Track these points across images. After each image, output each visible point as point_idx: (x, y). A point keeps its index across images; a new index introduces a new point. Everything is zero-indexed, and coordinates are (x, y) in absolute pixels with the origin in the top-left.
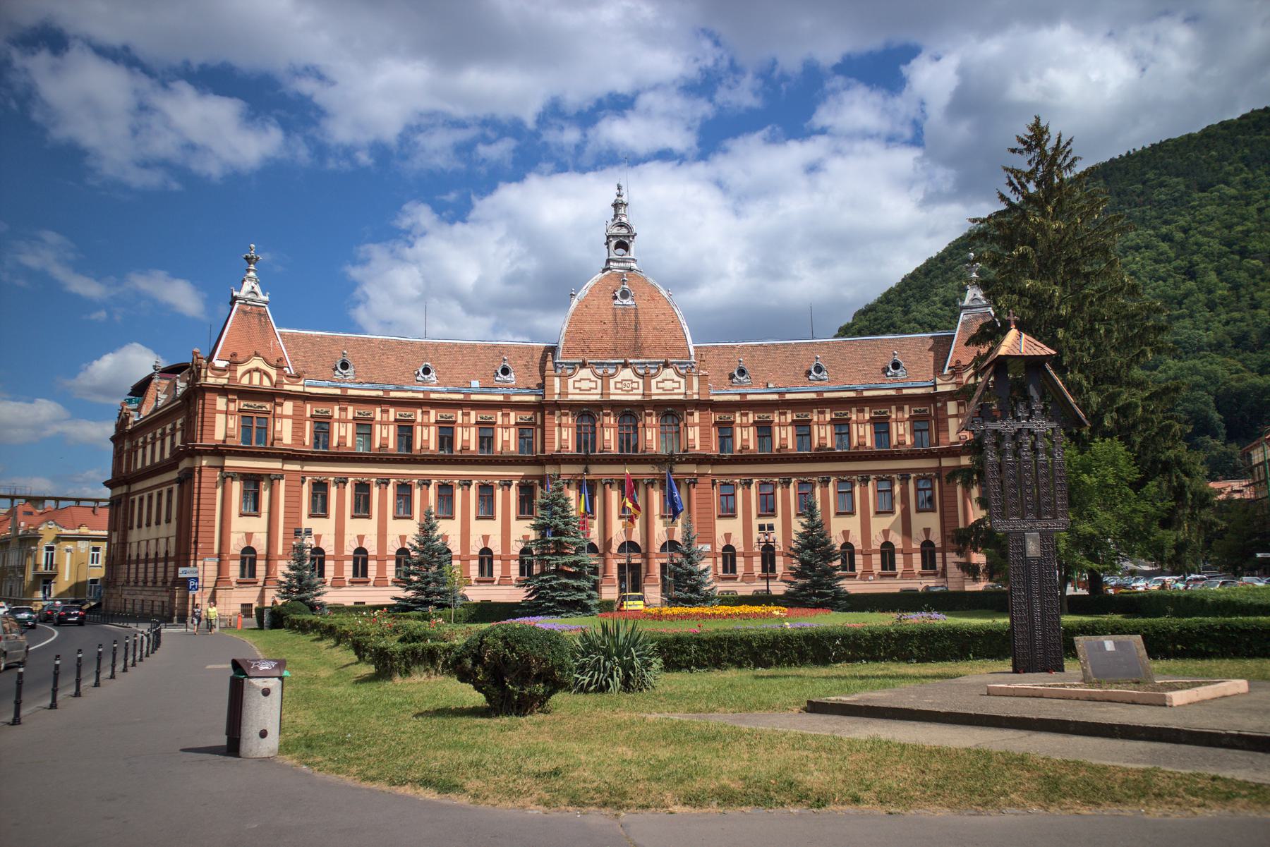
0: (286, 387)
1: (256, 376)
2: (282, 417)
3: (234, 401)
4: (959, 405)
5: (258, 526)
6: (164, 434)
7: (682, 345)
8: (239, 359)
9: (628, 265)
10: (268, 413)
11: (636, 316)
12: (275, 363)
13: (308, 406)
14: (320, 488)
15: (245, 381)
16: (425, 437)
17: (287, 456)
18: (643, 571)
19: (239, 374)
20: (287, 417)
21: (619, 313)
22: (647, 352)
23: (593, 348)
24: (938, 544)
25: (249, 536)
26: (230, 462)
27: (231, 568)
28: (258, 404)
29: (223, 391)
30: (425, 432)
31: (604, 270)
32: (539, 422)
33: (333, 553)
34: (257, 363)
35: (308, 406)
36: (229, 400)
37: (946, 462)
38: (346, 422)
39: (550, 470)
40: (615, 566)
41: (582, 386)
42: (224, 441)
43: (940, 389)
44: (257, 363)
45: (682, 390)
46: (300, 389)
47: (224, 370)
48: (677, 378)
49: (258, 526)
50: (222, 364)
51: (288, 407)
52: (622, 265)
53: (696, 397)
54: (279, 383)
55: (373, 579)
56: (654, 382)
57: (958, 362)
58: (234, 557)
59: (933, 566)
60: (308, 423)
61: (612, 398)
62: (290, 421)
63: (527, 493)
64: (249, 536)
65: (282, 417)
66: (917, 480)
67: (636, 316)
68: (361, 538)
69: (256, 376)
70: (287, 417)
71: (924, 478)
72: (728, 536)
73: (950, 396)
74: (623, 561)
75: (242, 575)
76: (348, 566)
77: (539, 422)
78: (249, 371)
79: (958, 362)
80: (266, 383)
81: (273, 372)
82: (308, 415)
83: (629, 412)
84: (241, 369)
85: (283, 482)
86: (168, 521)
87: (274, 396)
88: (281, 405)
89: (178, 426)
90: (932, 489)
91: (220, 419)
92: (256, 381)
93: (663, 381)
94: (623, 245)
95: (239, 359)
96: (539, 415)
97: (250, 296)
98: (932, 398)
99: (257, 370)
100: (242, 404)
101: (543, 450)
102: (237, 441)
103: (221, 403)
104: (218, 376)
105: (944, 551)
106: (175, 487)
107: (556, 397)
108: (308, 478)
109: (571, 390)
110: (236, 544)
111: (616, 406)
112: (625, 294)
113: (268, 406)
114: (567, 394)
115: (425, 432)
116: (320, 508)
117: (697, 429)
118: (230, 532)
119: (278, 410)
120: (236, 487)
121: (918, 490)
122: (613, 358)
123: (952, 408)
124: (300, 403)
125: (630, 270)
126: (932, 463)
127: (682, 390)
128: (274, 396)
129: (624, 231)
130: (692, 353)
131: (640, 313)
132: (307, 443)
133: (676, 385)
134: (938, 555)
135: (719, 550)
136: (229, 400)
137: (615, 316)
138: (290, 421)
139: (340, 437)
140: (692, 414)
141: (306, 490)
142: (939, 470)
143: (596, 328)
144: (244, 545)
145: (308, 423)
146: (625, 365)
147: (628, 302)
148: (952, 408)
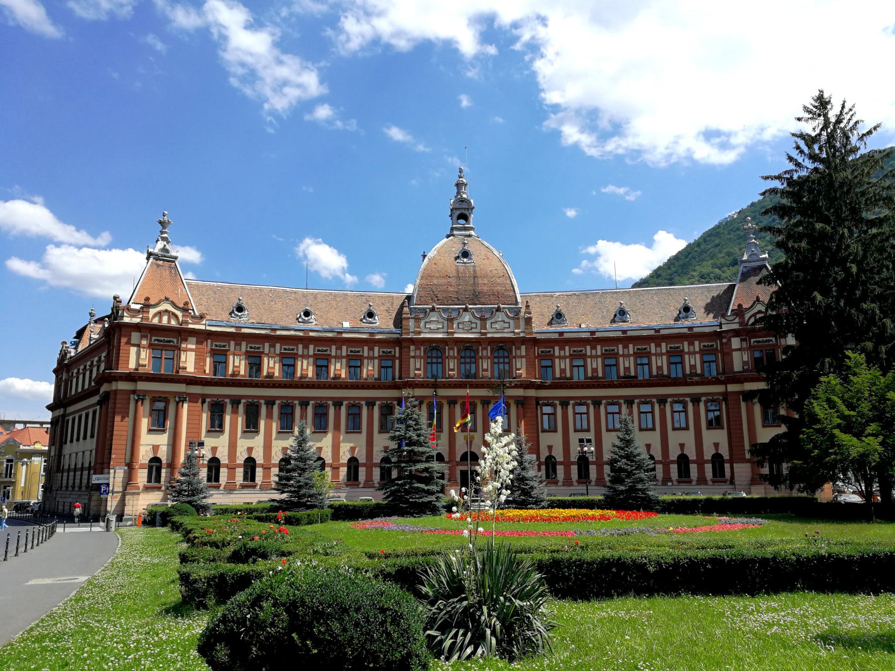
0: (190, 326)
3: (146, 337)
4: (742, 340)
5: (162, 440)
6: (92, 365)
7: (511, 293)
8: (152, 302)
9: (467, 233)
12: (181, 305)
15: (156, 321)
24: (726, 456)
27: (139, 475)
31: (448, 236)
32: (397, 355)
33: (227, 462)
37: (732, 388)
39: (405, 393)
42: (137, 369)
43: (725, 328)
46: (203, 327)
47: (138, 311)
48: (507, 320)
49: (162, 440)
50: (138, 307)
52: (463, 232)
53: (522, 335)
55: (259, 483)
57: (740, 306)
58: (142, 467)
59: (722, 474)
62: (194, 353)
63: (387, 410)
64: (156, 448)
65: (186, 350)
66: (706, 402)
68: (250, 450)
71: (713, 401)
72: (550, 448)
73: (736, 333)
75: (149, 481)
76: (240, 472)
78: (160, 314)
79: (740, 306)
80: (173, 323)
81: (179, 314)
83: (468, 347)
84: (152, 311)
86: (92, 436)
89: (103, 359)
90: (720, 410)
93: (496, 322)
94: (465, 217)
95: (152, 302)
96: (397, 349)
98: (717, 335)
99: (166, 311)
101: (400, 378)
102: (149, 369)
105: (731, 462)
106: (98, 407)
108: (208, 400)
110: (144, 454)
117: (524, 360)
118: (139, 445)
121: (707, 411)
123: (736, 343)
125: (470, 236)
126: (720, 389)
127: (511, 329)
129: (465, 205)
130: (519, 300)
132: (207, 371)
133: (507, 325)
134: (727, 466)
135: (543, 459)
138: (194, 353)
140: (519, 348)
142: (726, 395)
144: (151, 456)
146: (466, 310)
148: (736, 343)
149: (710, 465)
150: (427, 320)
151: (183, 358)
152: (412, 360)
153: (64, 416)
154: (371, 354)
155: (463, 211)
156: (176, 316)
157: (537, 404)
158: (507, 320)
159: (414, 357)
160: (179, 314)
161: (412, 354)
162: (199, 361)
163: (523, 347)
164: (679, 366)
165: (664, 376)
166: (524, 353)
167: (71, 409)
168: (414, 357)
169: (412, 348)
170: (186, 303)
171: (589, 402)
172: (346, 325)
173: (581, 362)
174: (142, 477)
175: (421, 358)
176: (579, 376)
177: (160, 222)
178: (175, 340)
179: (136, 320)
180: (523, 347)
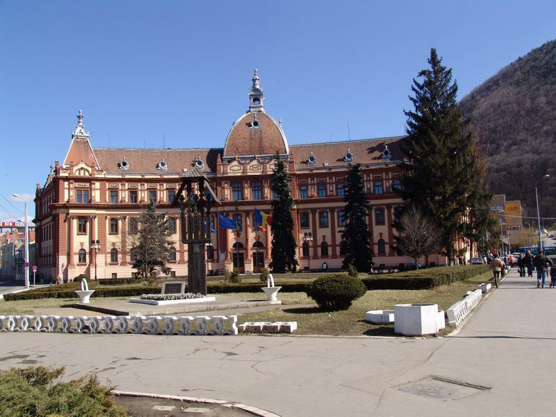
0: (96, 176)
2: (95, 189)
3: (72, 183)
8: (74, 164)
13: (107, 184)
15: (77, 174)
16: (162, 196)
18: (265, 255)
20: (98, 189)
22: (265, 151)
23: (240, 150)
26: (71, 211)
28: (84, 184)
30: (162, 193)
31: (247, 112)
35: (107, 184)
41: (234, 170)
44: (82, 165)
46: (103, 176)
49: (85, 239)
51: (97, 185)
52: (256, 109)
58: (76, 254)
60: (107, 192)
61: (249, 174)
65: (95, 189)
67: (261, 134)
69: (82, 171)
70: (98, 189)
74: (255, 251)
75: (80, 261)
80: (87, 174)
81: (90, 169)
84: (75, 169)
85: (96, 219)
87: (90, 180)
88: (94, 184)
91: (66, 192)
92: (82, 174)
97: (79, 134)
99: (82, 168)
100: (77, 185)
102: (74, 201)
109: (229, 171)
112: (256, 124)
113: (88, 185)
114: (227, 173)
120: (75, 223)
124: (102, 182)
130: (288, 150)
131: (263, 132)
132: (107, 201)
137: (251, 136)
143: (241, 141)
144: (80, 248)
145: (107, 192)
147: (257, 127)
149: (377, 246)
150: (232, 165)
151: (93, 194)
153: (41, 226)
156: (88, 172)
160: (90, 169)
164: (380, 188)
165: (371, 193)
167: (43, 222)
170: (93, 163)
171: (328, 210)
173: (380, 183)
174: (76, 259)
176: (379, 191)
179: (66, 175)
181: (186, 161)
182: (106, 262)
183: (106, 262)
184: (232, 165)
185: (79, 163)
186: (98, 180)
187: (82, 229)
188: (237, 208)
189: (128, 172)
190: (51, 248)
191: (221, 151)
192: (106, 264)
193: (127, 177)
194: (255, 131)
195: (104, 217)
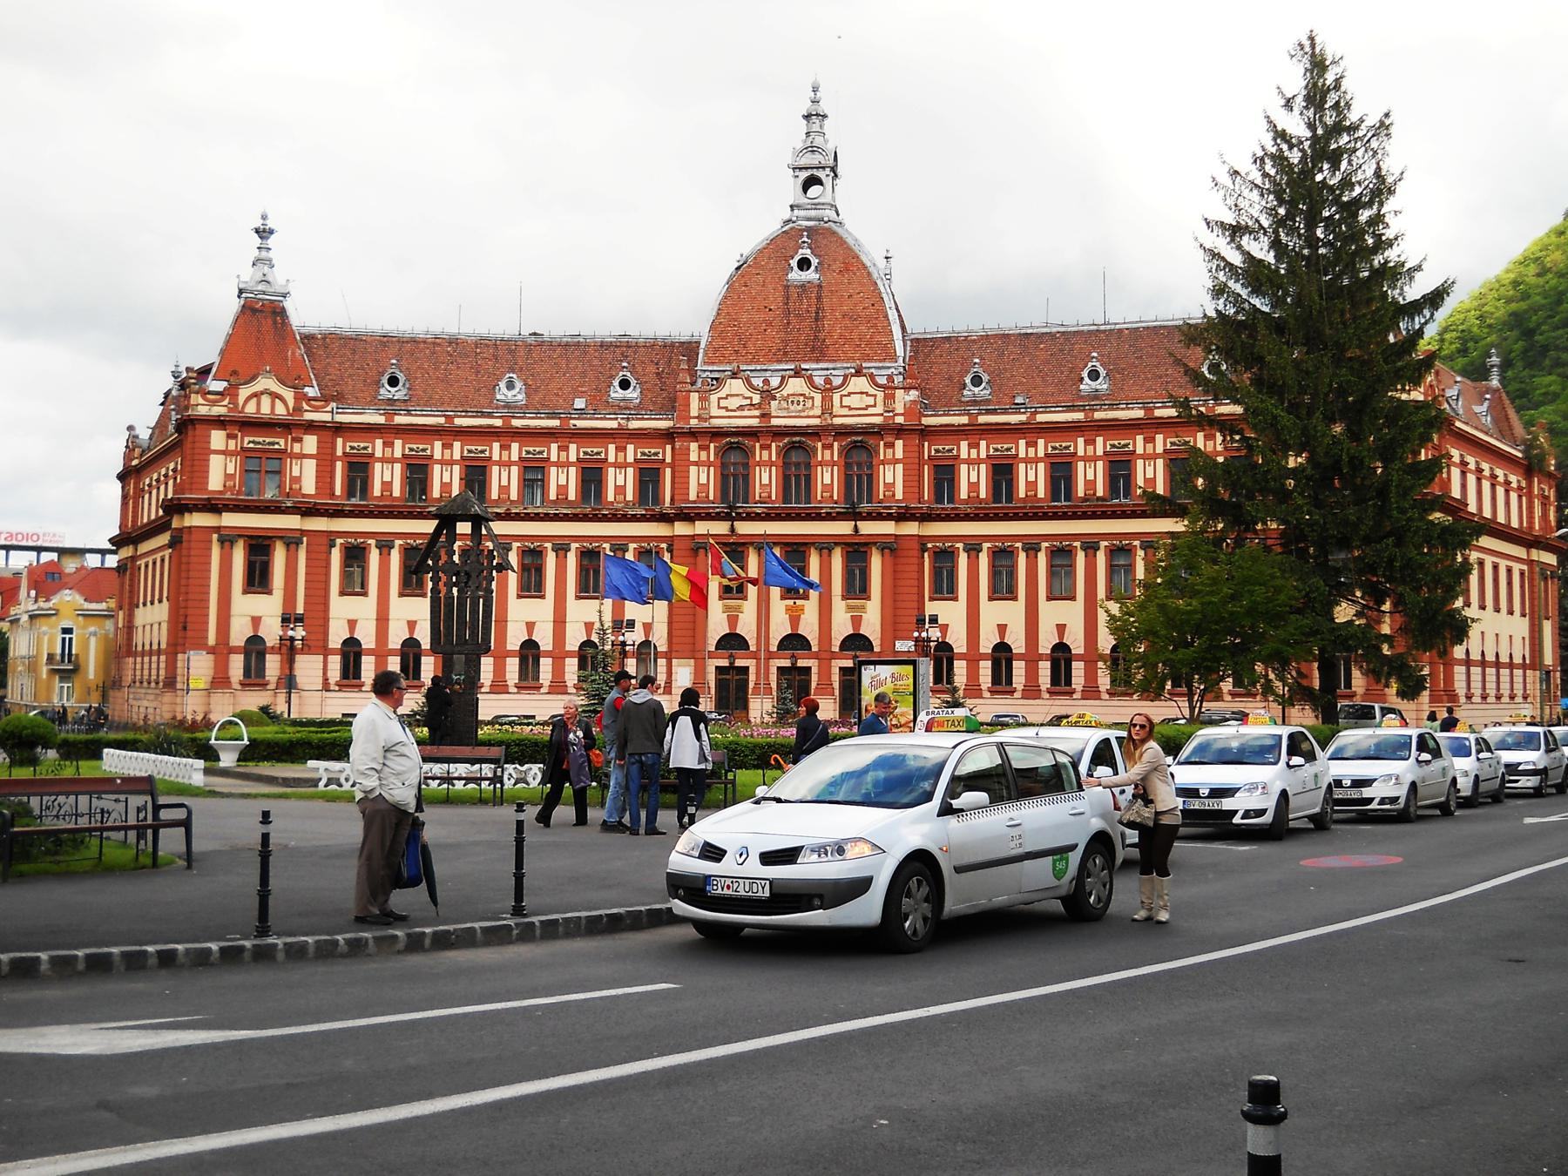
0: (309, 416)
1: (266, 400)
2: (302, 456)
3: (235, 437)
5: (268, 607)
7: (884, 340)
10: (284, 451)
11: (819, 298)
13: (340, 441)
14: (355, 555)
15: (251, 409)
17: (309, 510)
19: (241, 401)
21: (793, 293)
25: (256, 621)
29: (219, 422)
30: (505, 475)
32: (668, 460)
33: (372, 646)
34: (266, 383)
36: (229, 436)
38: (393, 461)
39: (681, 529)
40: (774, 670)
41: (730, 405)
45: (879, 409)
46: (327, 417)
51: (310, 443)
52: (813, 213)
53: (900, 420)
54: (298, 410)
56: (836, 397)
60: (339, 465)
65: (302, 456)
67: (819, 298)
69: (266, 400)
77: (668, 460)
78: (256, 395)
80: (280, 410)
81: (289, 395)
82: (339, 453)
84: (244, 393)
87: (291, 427)
88: (300, 440)
92: (266, 409)
93: (849, 394)
96: (668, 448)
97: (261, 287)
100: (248, 441)
103: (217, 439)
104: (214, 403)
107: (694, 422)
108: (339, 541)
110: (239, 633)
111: (842, 432)
113: (282, 443)
115: (505, 475)
116: (354, 585)
117: (900, 467)
119: (297, 448)
122: (779, 361)
124: (327, 435)
128: (291, 427)
132: (338, 492)
133: (871, 401)
136: (229, 436)
139: (383, 483)
140: (891, 445)
141: (336, 556)
143: (758, 317)
145: (339, 465)
147: (811, 275)
150: (722, 394)
152: (693, 469)
154: (621, 459)
155: (815, 172)
157: (924, 549)
158: (872, 391)
159: (696, 464)
161: (693, 457)
162: (324, 476)
163: (899, 444)
166: (899, 454)
168: (696, 464)
169: (694, 446)
172: (580, 403)
174: (237, 664)
175: (709, 464)
177: (257, 231)
178: (282, 442)
180: (899, 444)
181: (584, 374)
182: (326, 680)
183: (326, 680)
184: (722, 394)
185: (253, 378)
186: (311, 427)
187: (258, 579)
188: (732, 529)
189: (406, 406)
190: (165, 626)
191: (689, 349)
192: (326, 687)
193: (400, 420)
194: (804, 287)
195: (324, 540)
